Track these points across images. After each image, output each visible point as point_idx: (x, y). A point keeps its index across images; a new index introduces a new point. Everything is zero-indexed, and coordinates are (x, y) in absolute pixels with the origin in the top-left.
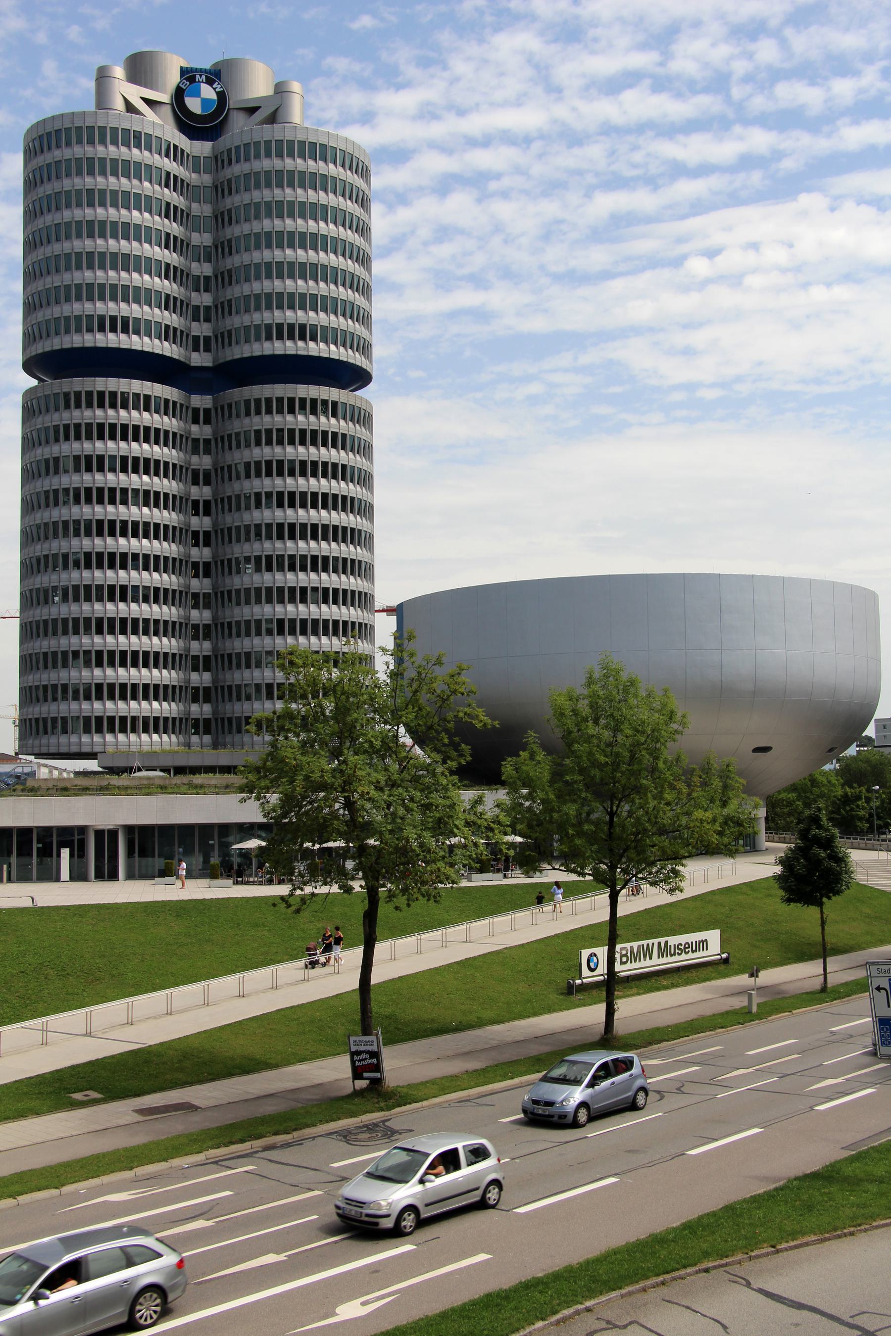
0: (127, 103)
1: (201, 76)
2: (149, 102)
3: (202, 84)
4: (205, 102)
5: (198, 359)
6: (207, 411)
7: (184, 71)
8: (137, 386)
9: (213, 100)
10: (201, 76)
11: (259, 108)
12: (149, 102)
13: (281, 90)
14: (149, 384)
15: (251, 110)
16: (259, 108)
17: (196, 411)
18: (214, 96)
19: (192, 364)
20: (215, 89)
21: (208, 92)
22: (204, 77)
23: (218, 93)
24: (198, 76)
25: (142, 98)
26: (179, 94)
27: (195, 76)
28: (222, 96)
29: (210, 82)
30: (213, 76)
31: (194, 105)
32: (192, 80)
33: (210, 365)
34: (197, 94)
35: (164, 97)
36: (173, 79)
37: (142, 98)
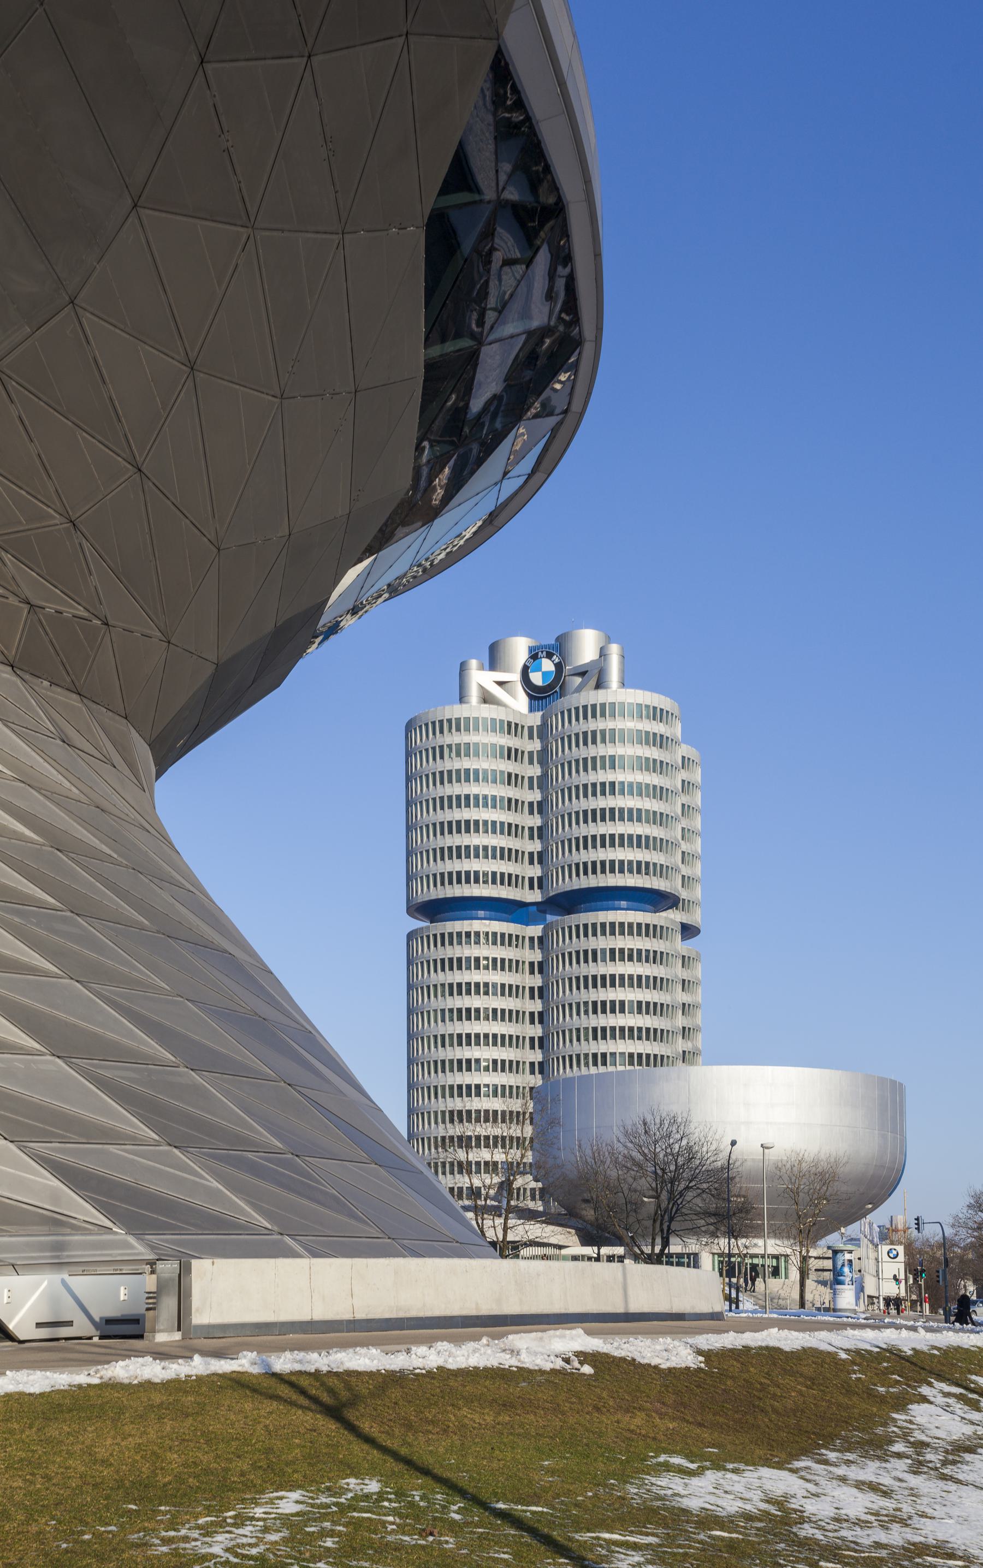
0: (481, 687)
2: (501, 684)
4: (545, 674)
7: (531, 649)
11: (586, 672)
12: (501, 684)
13: (603, 653)
15: (582, 674)
16: (586, 672)
18: (553, 668)
21: (548, 665)
23: (555, 665)
26: (525, 671)
28: (559, 667)
29: (549, 656)
31: (537, 679)
34: (539, 669)
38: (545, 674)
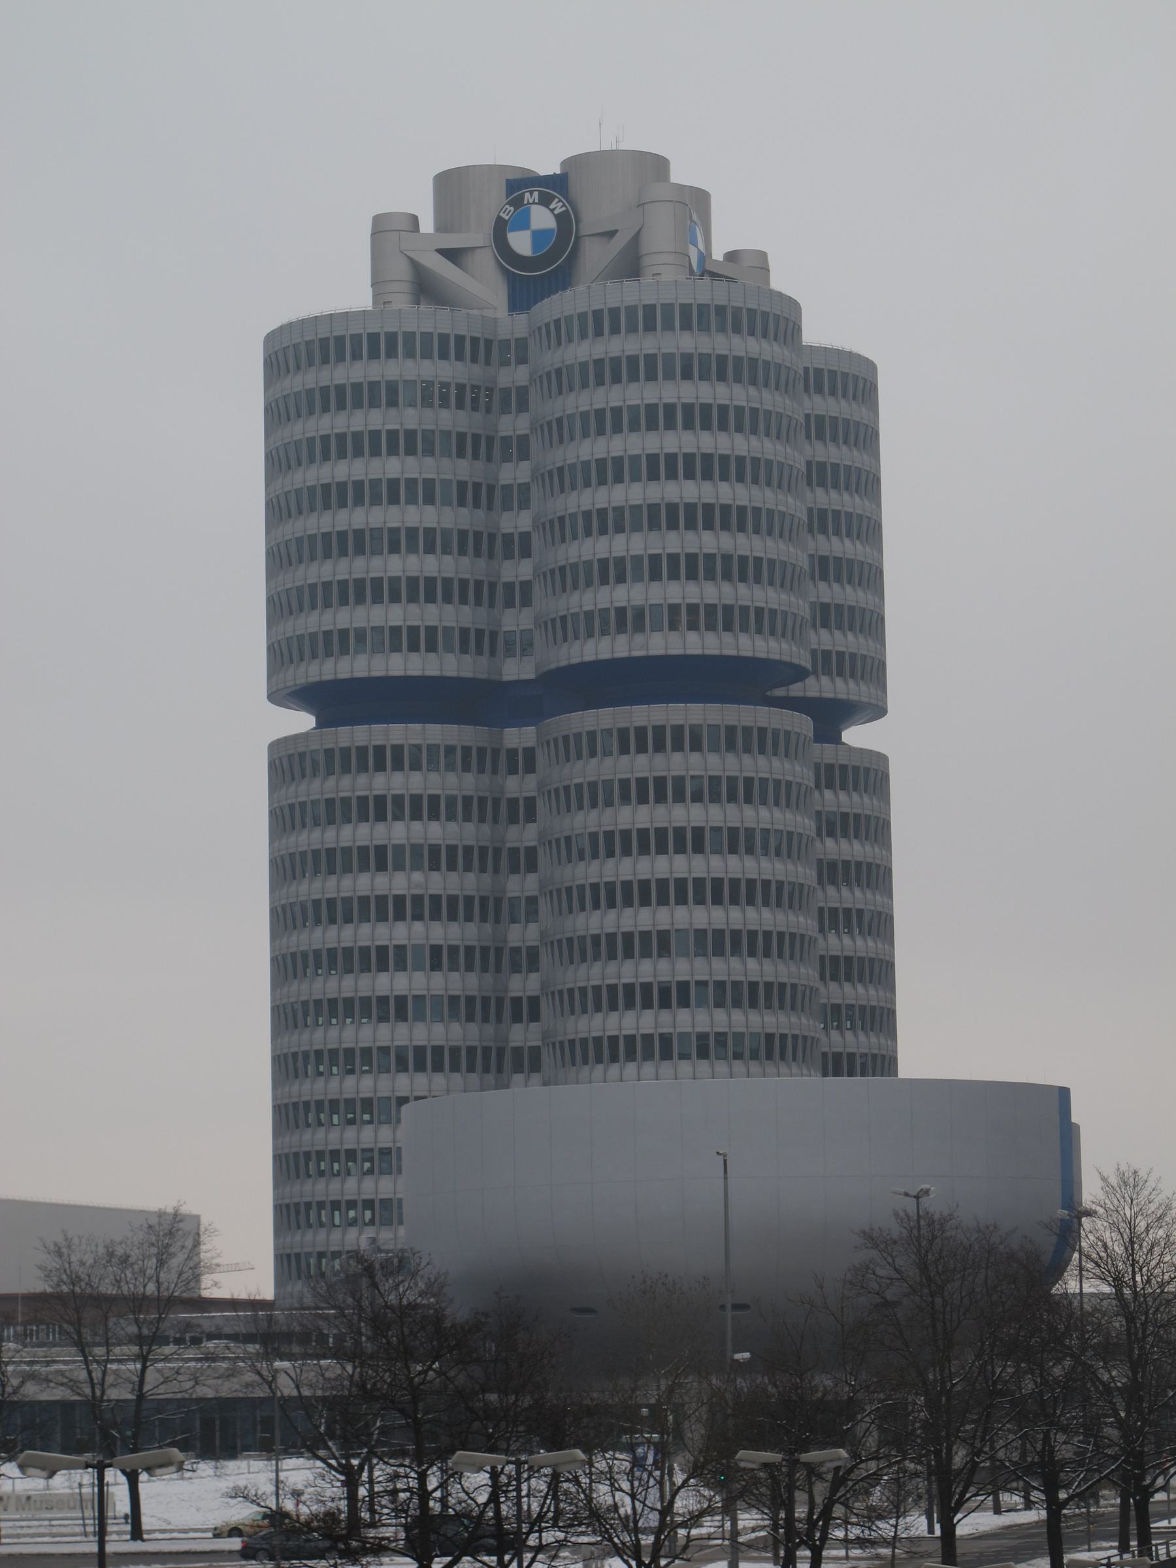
1: (531, 193)
3: (534, 207)
4: (539, 236)
5: (516, 670)
6: (530, 753)
8: (397, 734)
9: (552, 230)
10: (531, 193)
11: (616, 231)
14: (418, 726)
15: (612, 234)
16: (616, 231)
17: (512, 753)
19: (506, 678)
20: (552, 211)
21: (542, 218)
22: (536, 194)
23: (558, 217)
24: (527, 195)
25: (442, 252)
26: (500, 228)
27: (523, 194)
28: (562, 219)
29: (545, 201)
30: (554, 187)
31: (521, 243)
32: (517, 203)
33: (532, 676)
34: (523, 223)
35: (477, 236)
36: (494, 202)
37: (442, 252)
38: (539, 236)
